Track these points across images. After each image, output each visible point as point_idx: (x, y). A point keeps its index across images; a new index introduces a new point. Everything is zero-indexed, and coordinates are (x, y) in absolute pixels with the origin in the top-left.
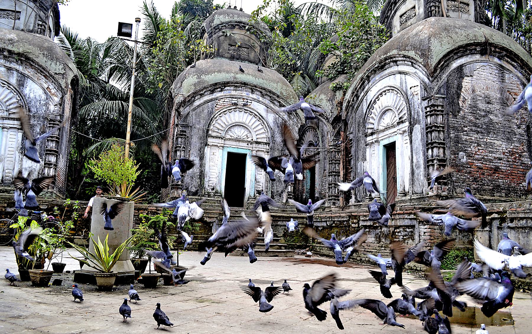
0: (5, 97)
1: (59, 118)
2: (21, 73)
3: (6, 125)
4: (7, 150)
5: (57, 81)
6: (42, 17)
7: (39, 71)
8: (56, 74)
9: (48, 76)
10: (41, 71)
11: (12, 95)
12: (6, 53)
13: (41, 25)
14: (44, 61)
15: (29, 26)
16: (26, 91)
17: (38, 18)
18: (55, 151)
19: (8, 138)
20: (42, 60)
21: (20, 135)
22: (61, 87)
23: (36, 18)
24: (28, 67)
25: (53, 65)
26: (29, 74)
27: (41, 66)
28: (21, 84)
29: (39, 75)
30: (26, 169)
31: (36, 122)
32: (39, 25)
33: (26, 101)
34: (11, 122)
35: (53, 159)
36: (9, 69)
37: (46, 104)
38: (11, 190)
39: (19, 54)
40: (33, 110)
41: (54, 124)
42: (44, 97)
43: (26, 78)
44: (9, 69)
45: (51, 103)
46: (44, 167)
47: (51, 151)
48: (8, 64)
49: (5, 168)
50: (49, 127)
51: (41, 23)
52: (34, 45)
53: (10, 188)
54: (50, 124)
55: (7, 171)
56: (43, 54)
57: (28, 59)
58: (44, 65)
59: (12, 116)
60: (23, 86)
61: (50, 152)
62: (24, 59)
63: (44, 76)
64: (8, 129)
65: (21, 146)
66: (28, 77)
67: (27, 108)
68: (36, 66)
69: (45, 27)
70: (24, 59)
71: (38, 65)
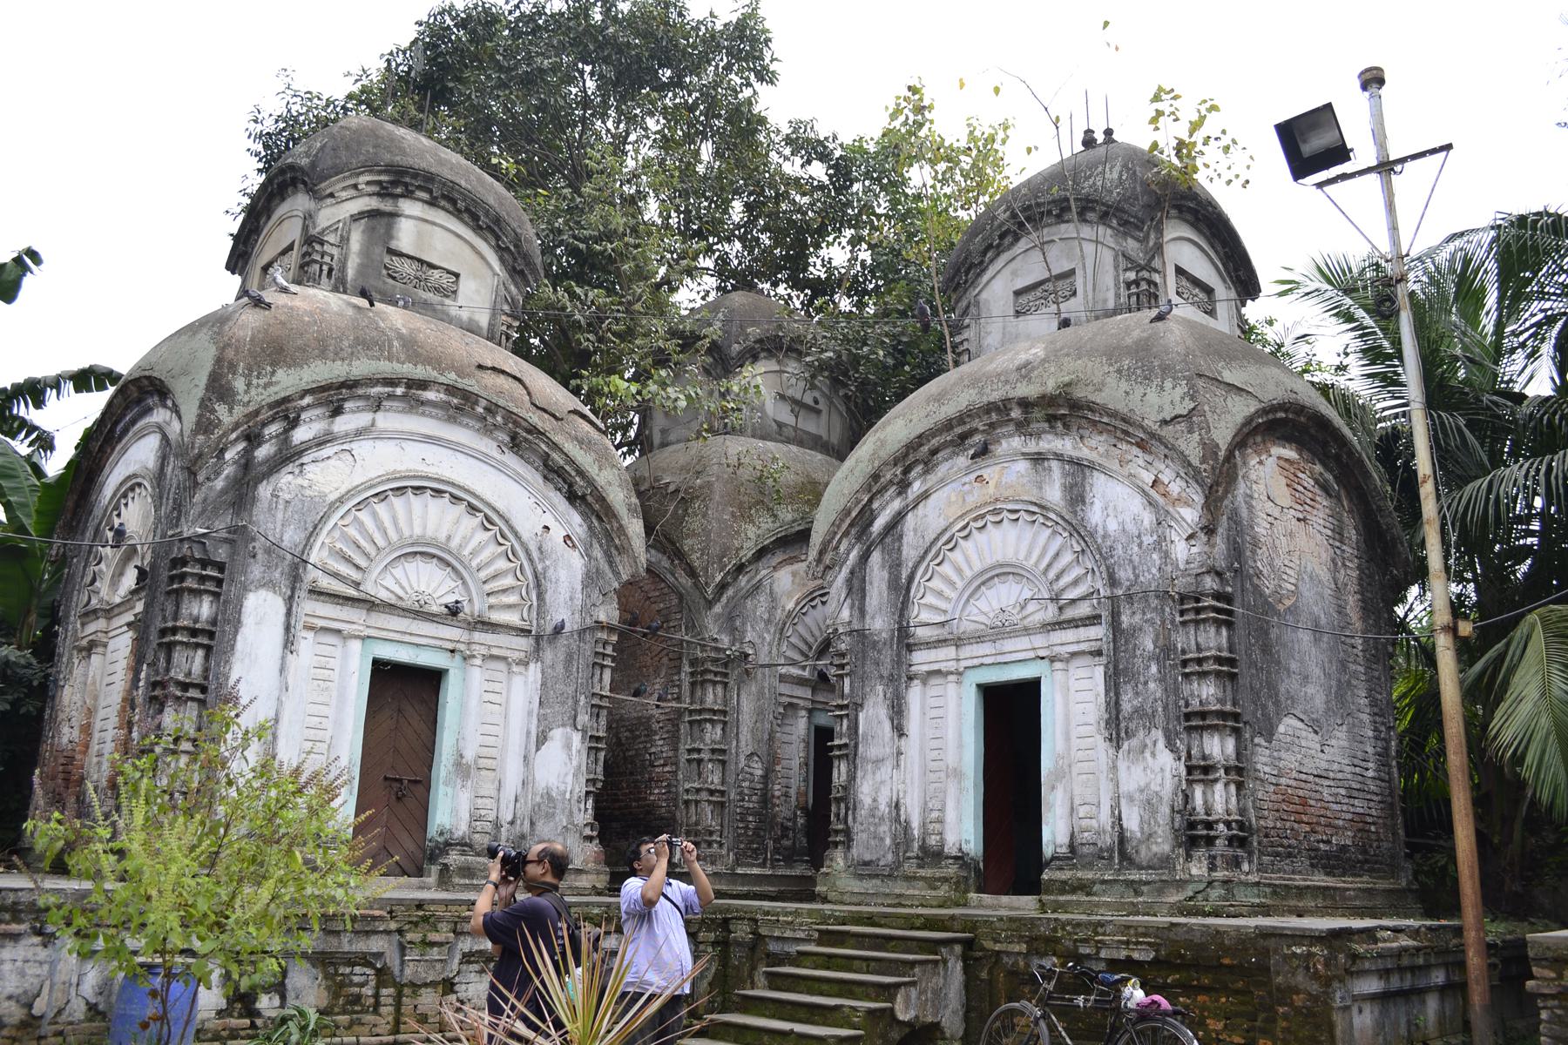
0: (1042, 555)
1: (1210, 583)
2: (1071, 461)
3: (1057, 649)
4: (1074, 735)
5: (1173, 448)
6: (1133, 254)
7: (1118, 433)
8: (1165, 422)
9: (1147, 442)
10: (1126, 433)
11: (1058, 542)
12: (1016, 413)
13: (1137, 283)
14: (1121, 392)
15: (1105, 301)
16: (1095, 515)
17: (1123, 263)
18: (1222, 715)
19: (1072, 691)
20: (1113, 393)
21: (1099, 672)
22: (1190, 464)
23: (1116, 267)
24: (1086, 433)
25: (1152, 396)
26: (1093, 456)
27: (1114, 414)
28: (1077, 497)
29: (1124, 446)
30: (1131, 799)
31: (1138, 617)
32: (1128, 285)
33: (1099, 549)
34: (1069, 635)
35: (1219, 747)
36: (1038, 459)
37: (1161, 544)
38: (1094, 882)
39: (1047, 401)
40: (1124, 574)
41: (1198, 611)
42: (1148, 518)
43: (1087, 472)
44: (1038, 459)
45: (1175, 538)
46: (1190, 783)
47: (1203, 715)
48: (1032, 446)
49: (1077, 802)
50: (1184, 623)
51: (1132, 276)
52: (1091, 354)
53: (1090, 875)
54: (1182, 613)
55: (1082, 812)
56: (1119, 371)
57: (1076, 406)
58: (1122, 408)
59: (1069, 613)
60: (1084, 502)
61: (1197, 721)
62: (1063, 409)
63: (1138, 445)
64: (1067, 661)
65: (1106, 716)
66: (1092, 467)
67: (1105, 575)
68: (1105, 420)
69: (1150, 282)
70: (1063, 409)
71: (1108, 415)
